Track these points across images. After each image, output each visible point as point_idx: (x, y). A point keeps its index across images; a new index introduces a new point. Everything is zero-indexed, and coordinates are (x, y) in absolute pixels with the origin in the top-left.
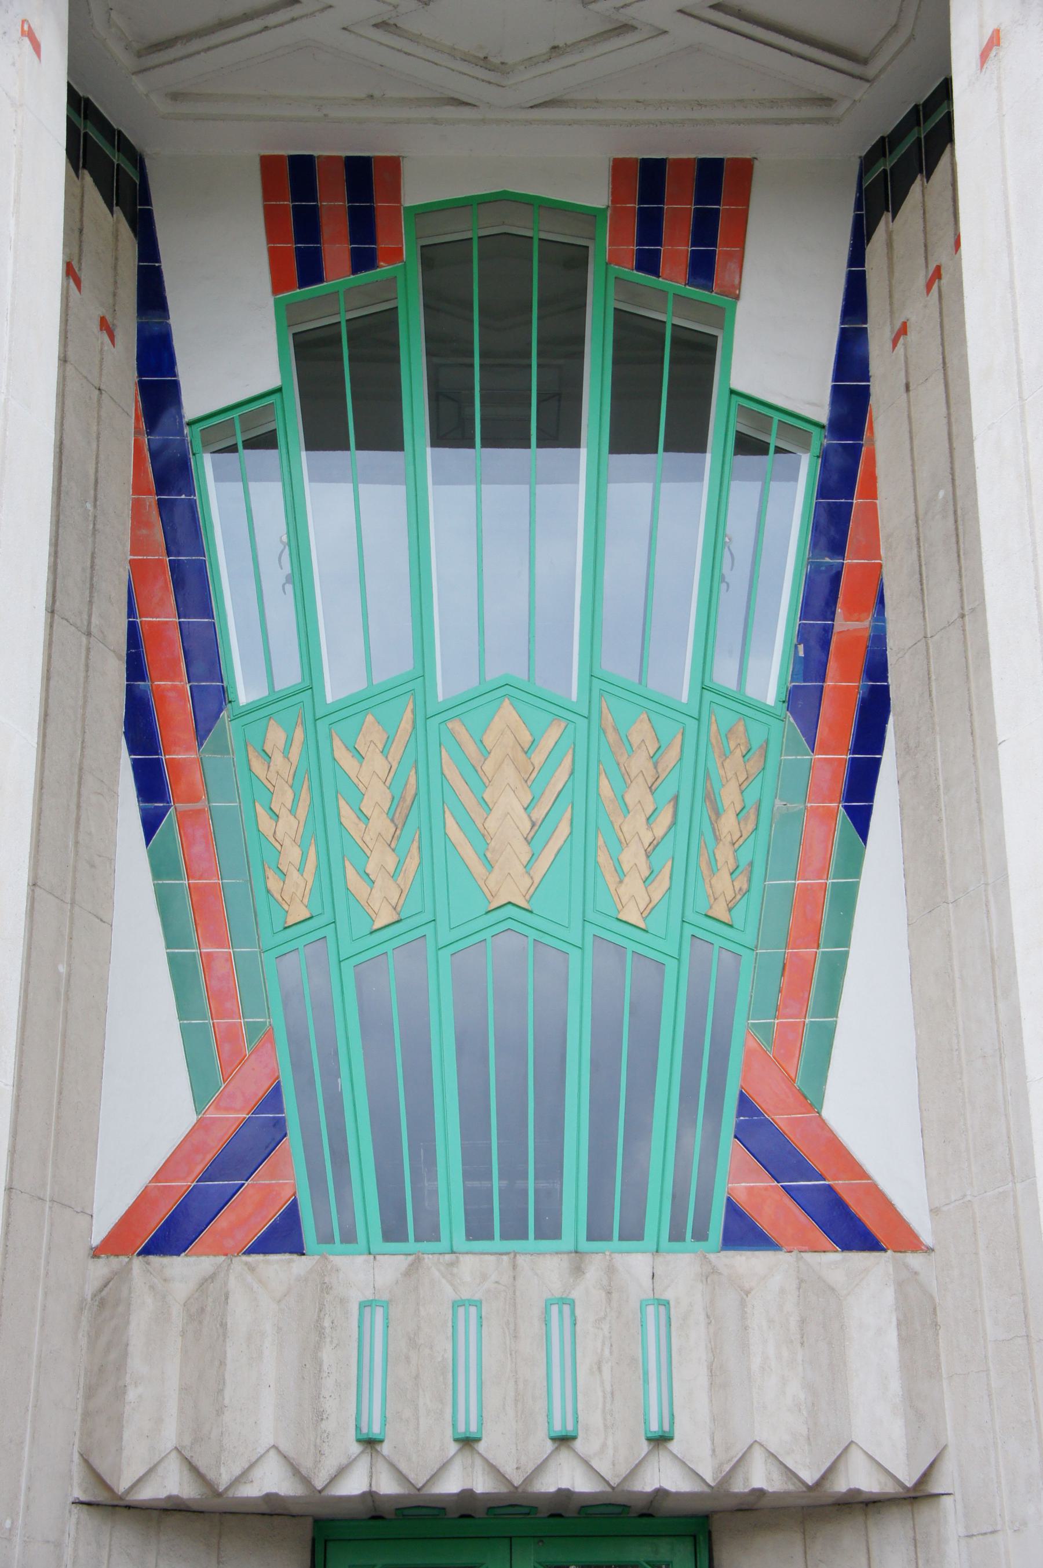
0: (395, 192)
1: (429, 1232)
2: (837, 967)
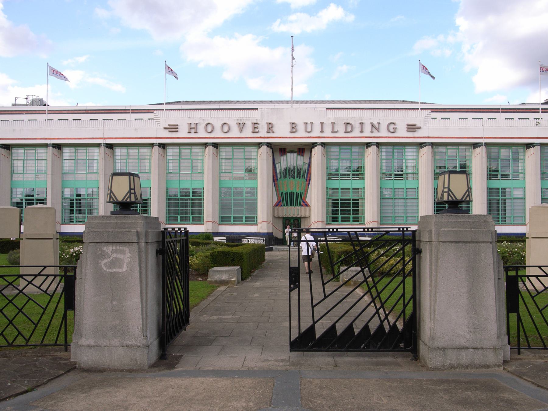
0: (286, 150)
1: (288, 205)
2: (307, 193)
